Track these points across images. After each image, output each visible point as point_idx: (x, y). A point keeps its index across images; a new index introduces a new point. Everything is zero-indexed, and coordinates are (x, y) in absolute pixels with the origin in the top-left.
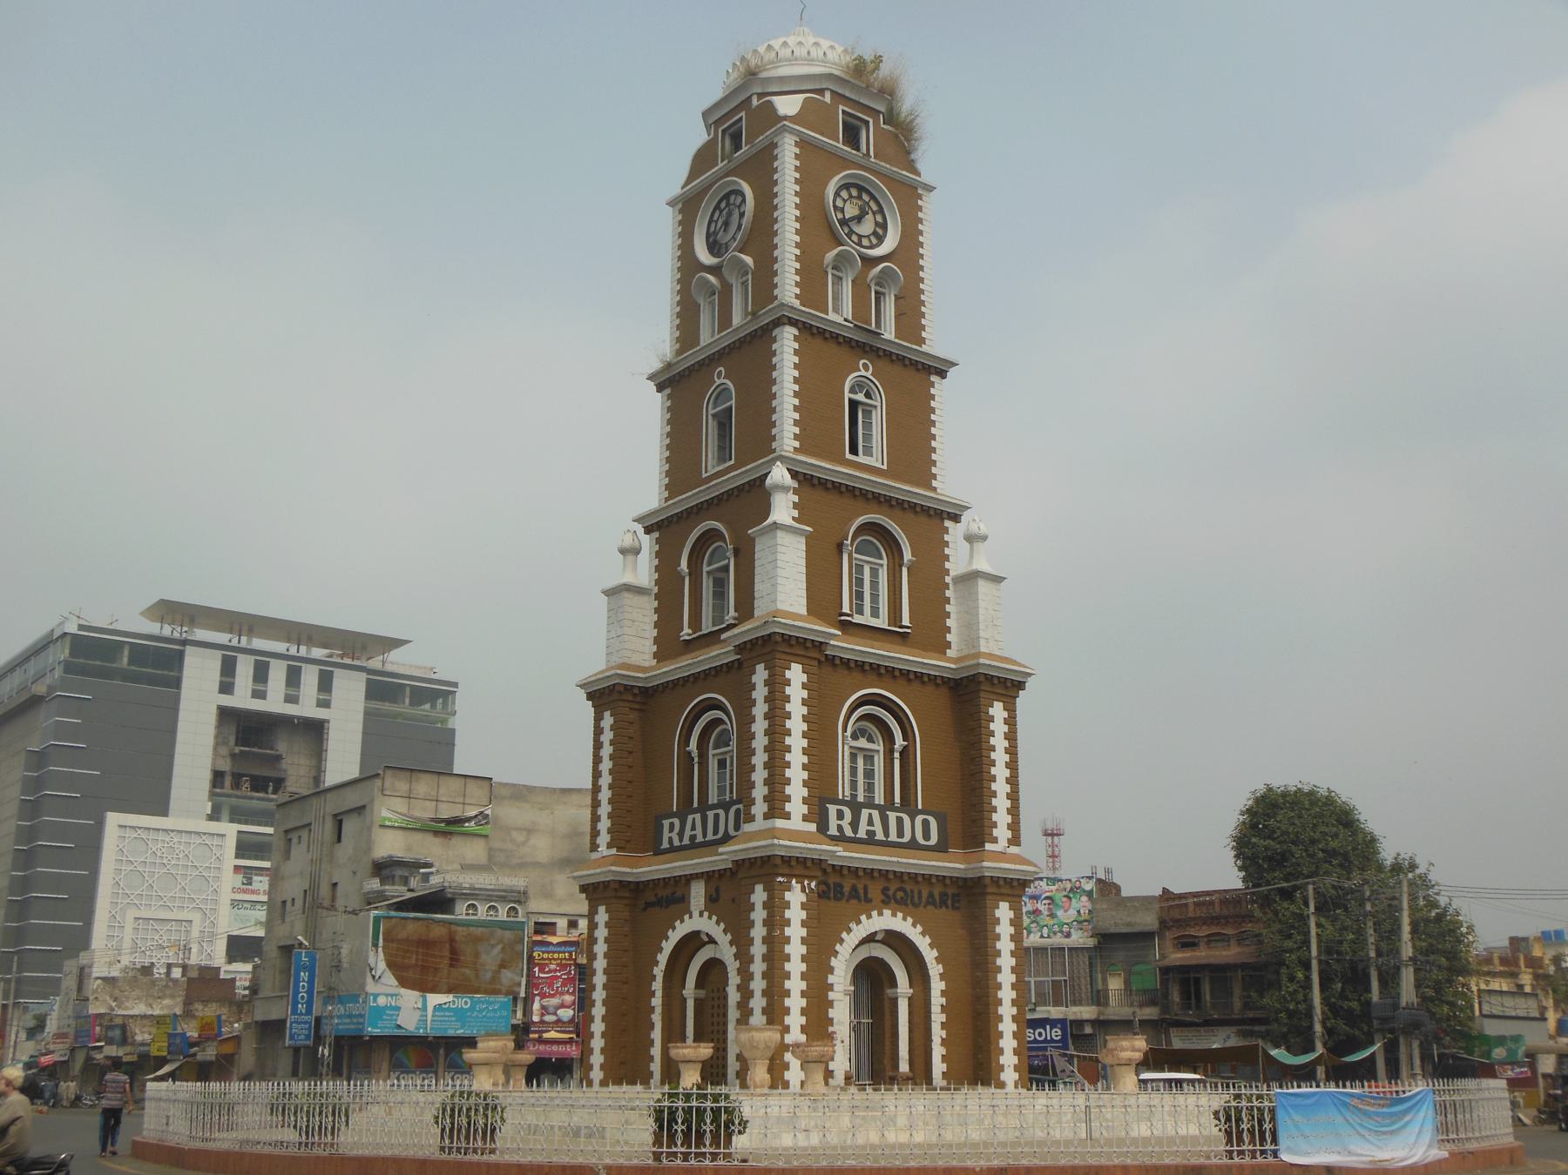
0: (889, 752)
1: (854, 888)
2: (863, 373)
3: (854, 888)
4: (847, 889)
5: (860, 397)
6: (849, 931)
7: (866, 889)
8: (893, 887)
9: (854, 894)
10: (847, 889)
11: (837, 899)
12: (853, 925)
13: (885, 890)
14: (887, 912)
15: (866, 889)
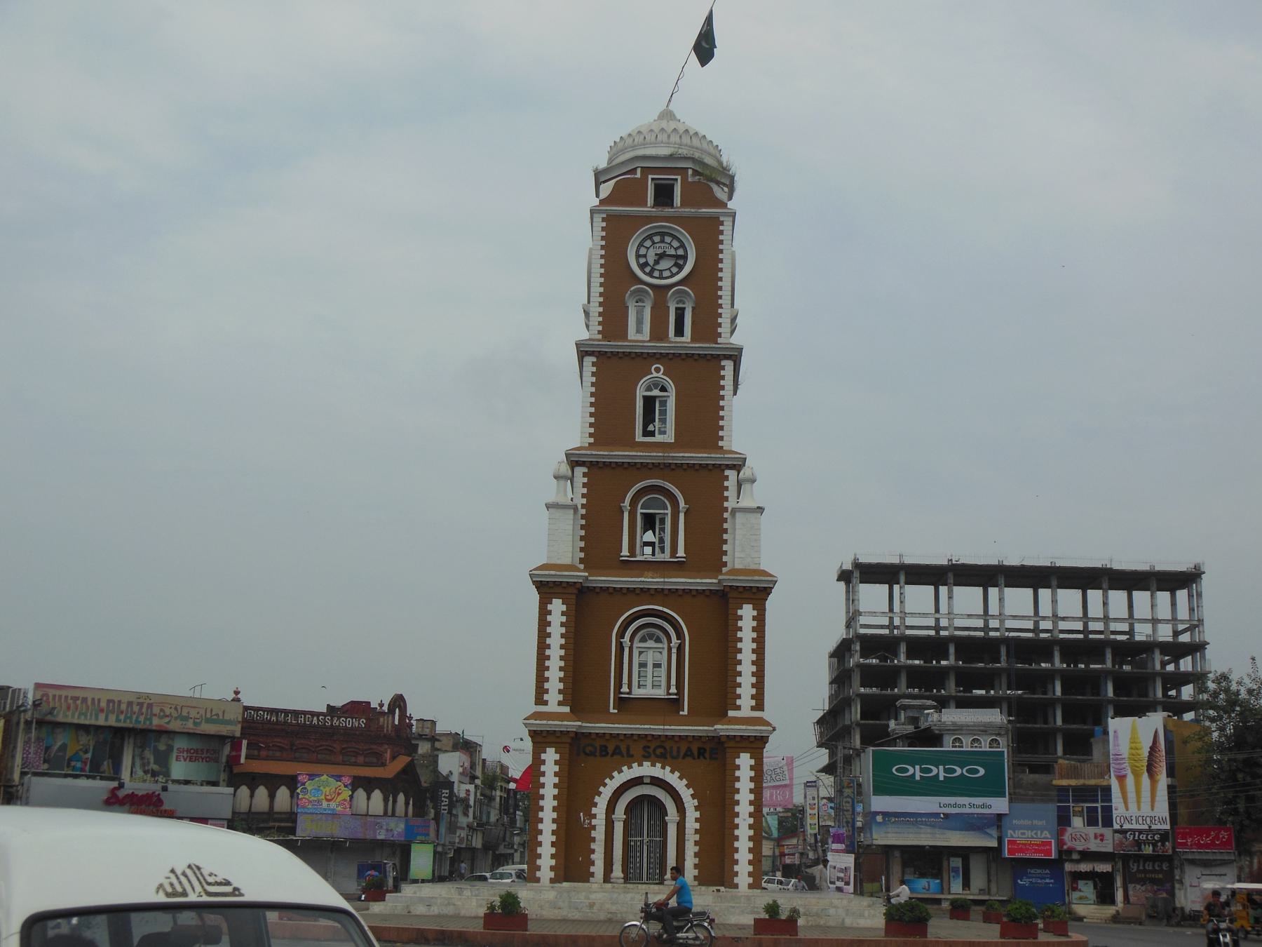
0: (670, 649)
1: (617, 748)
2: (655, 374)
3: (617, 748)
4: (611, 749)
5: (656, 392)
6: (612, 778)
7: (628, 749)
8: (653, 745)
9: (617, 751)
10: (611, 749)
11: (602, 756)
12: (615, 774)
13: (646, 748)
14: (659, 765)
15: (628, 749)
